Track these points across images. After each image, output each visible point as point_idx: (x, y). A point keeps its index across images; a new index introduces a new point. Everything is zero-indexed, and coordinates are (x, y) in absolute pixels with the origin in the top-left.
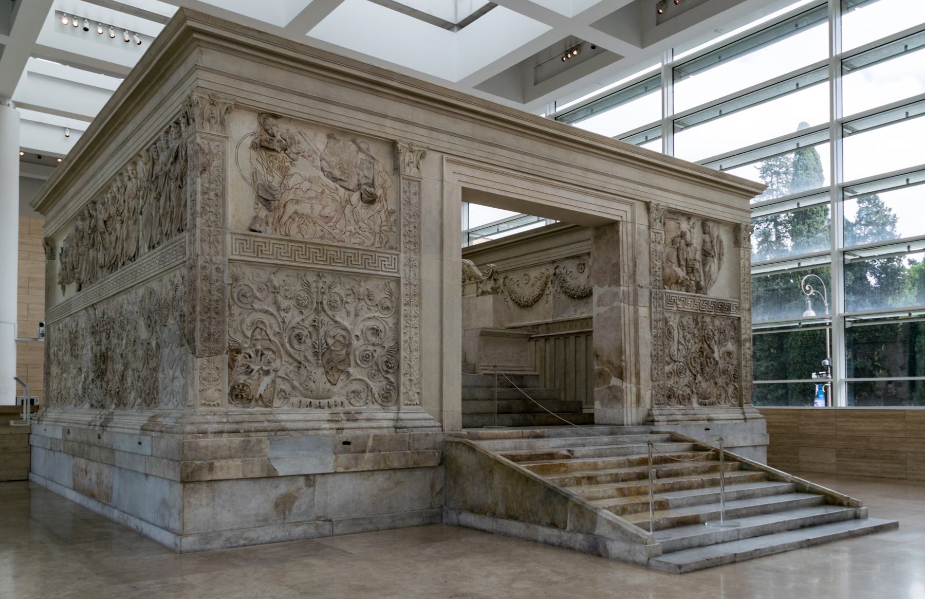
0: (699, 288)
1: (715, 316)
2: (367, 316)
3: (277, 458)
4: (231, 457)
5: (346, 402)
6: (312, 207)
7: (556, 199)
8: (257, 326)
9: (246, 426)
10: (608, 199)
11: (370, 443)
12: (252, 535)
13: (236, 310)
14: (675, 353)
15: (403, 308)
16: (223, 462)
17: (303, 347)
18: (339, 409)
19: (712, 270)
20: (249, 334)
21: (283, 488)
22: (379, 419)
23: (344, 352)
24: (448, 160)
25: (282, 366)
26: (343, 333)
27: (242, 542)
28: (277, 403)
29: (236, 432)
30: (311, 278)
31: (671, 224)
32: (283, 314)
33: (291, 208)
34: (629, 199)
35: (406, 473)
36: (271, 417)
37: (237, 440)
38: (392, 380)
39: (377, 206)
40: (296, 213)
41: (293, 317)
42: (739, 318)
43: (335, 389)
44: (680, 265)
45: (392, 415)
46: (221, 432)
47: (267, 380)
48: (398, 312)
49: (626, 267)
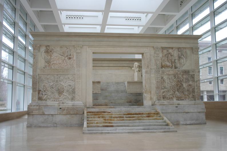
0: (176, 68)
2: (68, 82)
3: (45, 111)
4: (36, 110)
5: (63, 100)
6: (57, 62)
8: (44, 86)
9: (40, 105)
12: (40, 125)
13: (40, 83)
14: (166, 86)
15: (76, 80)
16: (35, 111)
17: (53, 90)
18: (61, 101)
20: (42, 87)
21: (46, 117)
22: (69, 103)
23: (63, 90)
24: (88, 47)
25: (49, 93)
26: (62, 86)
27: (38, 126)
28: (48, 100)
30: (55, 76)
32: (49, 83)
33: (52, 63)
35: (75, 115)
36: (46, 103)
37: (37, 107)
38: (74, 95)
39: (72, 59)
40: (53, 63)
41: (52, 84)
42: (194, 75)
43: (60, 97)
44: (168, 61)
45: (73, 103)
46: (35, 106)
47: (46, 96)
48: (75, 81)
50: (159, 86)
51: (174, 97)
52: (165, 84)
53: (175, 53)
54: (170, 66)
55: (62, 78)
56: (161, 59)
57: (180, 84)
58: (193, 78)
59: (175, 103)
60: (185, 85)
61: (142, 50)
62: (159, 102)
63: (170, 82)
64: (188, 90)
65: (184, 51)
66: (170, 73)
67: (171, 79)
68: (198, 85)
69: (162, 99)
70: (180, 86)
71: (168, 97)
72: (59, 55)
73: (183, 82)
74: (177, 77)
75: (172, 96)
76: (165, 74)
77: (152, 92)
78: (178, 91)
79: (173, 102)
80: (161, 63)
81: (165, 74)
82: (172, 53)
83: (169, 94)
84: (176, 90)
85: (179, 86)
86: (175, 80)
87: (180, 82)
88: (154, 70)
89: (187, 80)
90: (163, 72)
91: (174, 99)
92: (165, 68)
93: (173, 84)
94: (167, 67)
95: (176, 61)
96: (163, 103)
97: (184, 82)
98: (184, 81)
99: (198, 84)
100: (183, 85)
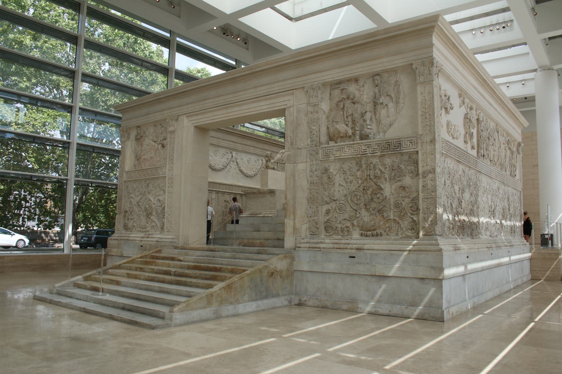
0: (364, 137)
1: (382, 156)
2: (157, 194)
7: (240, 112)
10: (275, 98)
11: (148, 247)
14: (336, 193)
18: (148, 233)
19: (382, 115)
24: (187, 117)
29: (117, 239)
31: (337, 92)
34: (290, 91)
43: (147, 225)
47: (132, 222)
49: (289, 138)
50: (316, 195)
51: (353, 225)
52: (333, 189)
53: (365, 92)
54: (348, 135)
55: (150, 186)
56: (327, 118)
57: (374, 186)
58: (416, 163)
59: (349, 246)
60: (388, 189)
61: (278, 103)
62: (312, 241)
63: (346, 182)
64: (397, 205)
65: (393, 80)
66: (343, 155)
67: (348, 173)
68: (429, 186)
69: (324, 232)
70: (374, 193)
71: (339, 226)
72: (151, 141)
73: (383, 179)
74: (364, 166)
75: (348, 224)
76: (332, 158)
77: (299, 213)
78: (367, 210)
79: (347, 241)
80: (328, 128)
81: (332, 158)
82: (357, 94)
83: (341, 219)
84: (362, 204)
85: (369, 192)
86: (359, 173)
87: (375, 180)
88: (304, 152)
89: (397, 174)
90: (327, 155)
91: (354, 232)
92: (336, 143)
93: (353, 188)
94: (342, 137)
95: (368, 116)
96: (321, 243)
97: (386, 179)
98: (387, 176)
99: (429, 182)
100: (381, 189)
